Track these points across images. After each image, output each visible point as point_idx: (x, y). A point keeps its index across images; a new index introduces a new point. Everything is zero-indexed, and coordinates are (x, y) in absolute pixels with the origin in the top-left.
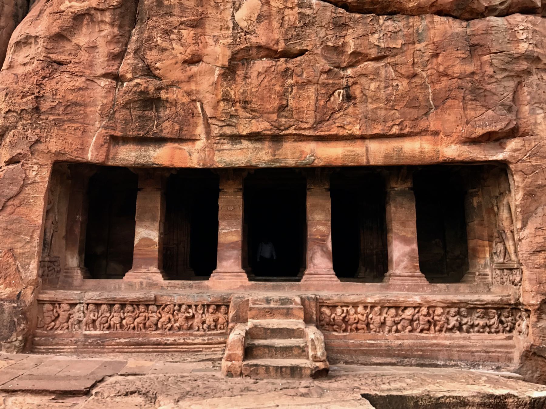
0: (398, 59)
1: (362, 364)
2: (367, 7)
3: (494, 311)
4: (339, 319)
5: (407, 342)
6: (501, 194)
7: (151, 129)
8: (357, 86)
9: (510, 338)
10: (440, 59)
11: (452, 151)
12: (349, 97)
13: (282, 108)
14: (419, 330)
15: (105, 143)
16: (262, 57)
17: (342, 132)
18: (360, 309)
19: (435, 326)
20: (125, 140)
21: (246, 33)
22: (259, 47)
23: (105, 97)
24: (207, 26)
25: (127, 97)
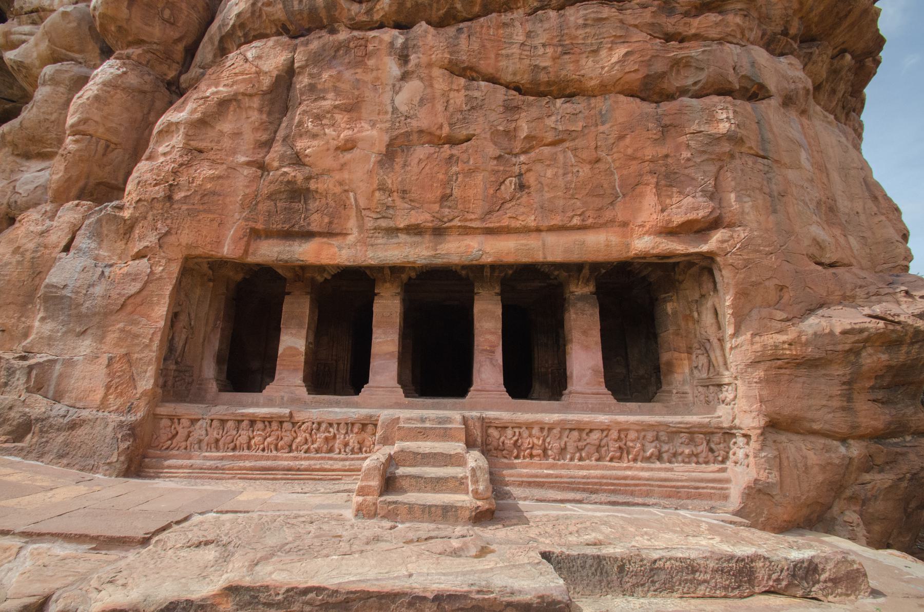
0: (579, 143)
1: (538, 500)
2: (542, 89)
3: (702, 436)
4: (509, 443)
5: (593, 472)
6: (703, 296)
7: (297, 223)
8: (531, 173)
9: (724, 470)
10: (627, 141)
11: (644, 244)
12: (522, 187)
13: (445, 198)
14: (608, 459)
15: (245, 236)
16: (423, 144)
17: (514, 224)
18: (535, 431)
19: (628, 453)
20: (269, 234)
21: (407, 117)
22: (421, 132)
23: (247, 187)
24: (363, 110)
25: (273, 187)
